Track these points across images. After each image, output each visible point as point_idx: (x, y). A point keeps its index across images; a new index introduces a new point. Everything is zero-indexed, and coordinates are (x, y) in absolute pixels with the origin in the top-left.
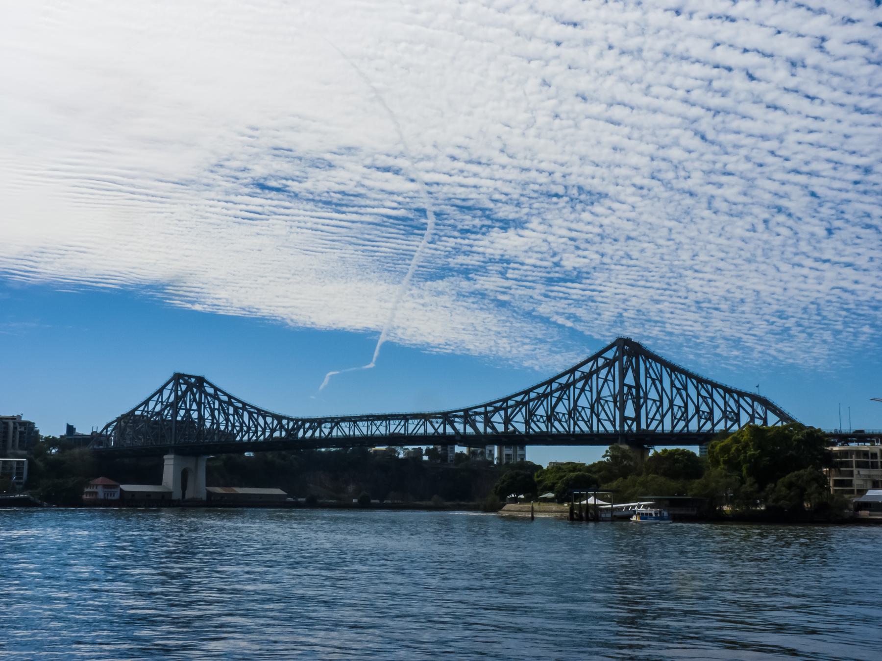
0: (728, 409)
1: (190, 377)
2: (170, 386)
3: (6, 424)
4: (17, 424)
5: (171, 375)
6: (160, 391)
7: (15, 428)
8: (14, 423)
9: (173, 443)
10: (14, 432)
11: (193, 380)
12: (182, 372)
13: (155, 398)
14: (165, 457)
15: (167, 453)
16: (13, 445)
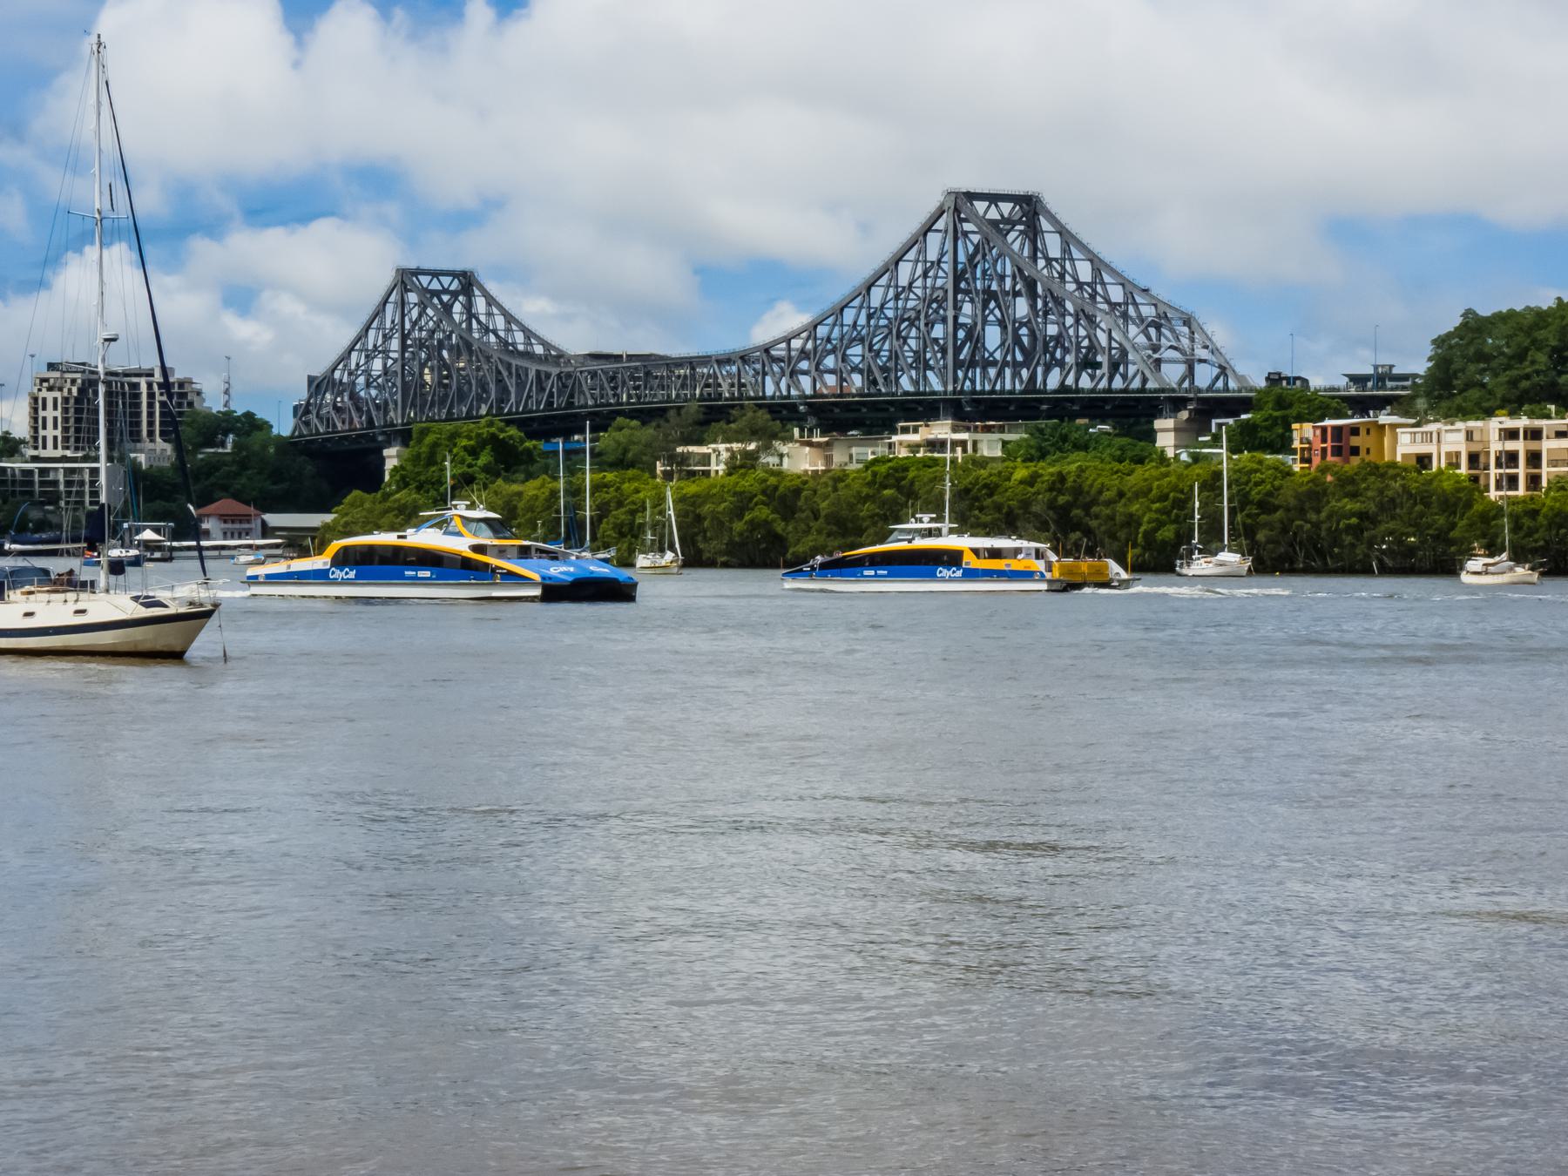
0: (1114, 344)
1: (435, 274)
2: (392, 299)
3: (136, 386)
4: (155, 387)
5: (387, 278)
6: (380, 311)
7: (151, 395)
8: (150, 385)
9: (400, 421)
10: (151, 405)
11: (446, 280)
12: (413, 265)
13: (375, 325)
14: (386, 452)
15: (389, 444)
16: (151, 434)
